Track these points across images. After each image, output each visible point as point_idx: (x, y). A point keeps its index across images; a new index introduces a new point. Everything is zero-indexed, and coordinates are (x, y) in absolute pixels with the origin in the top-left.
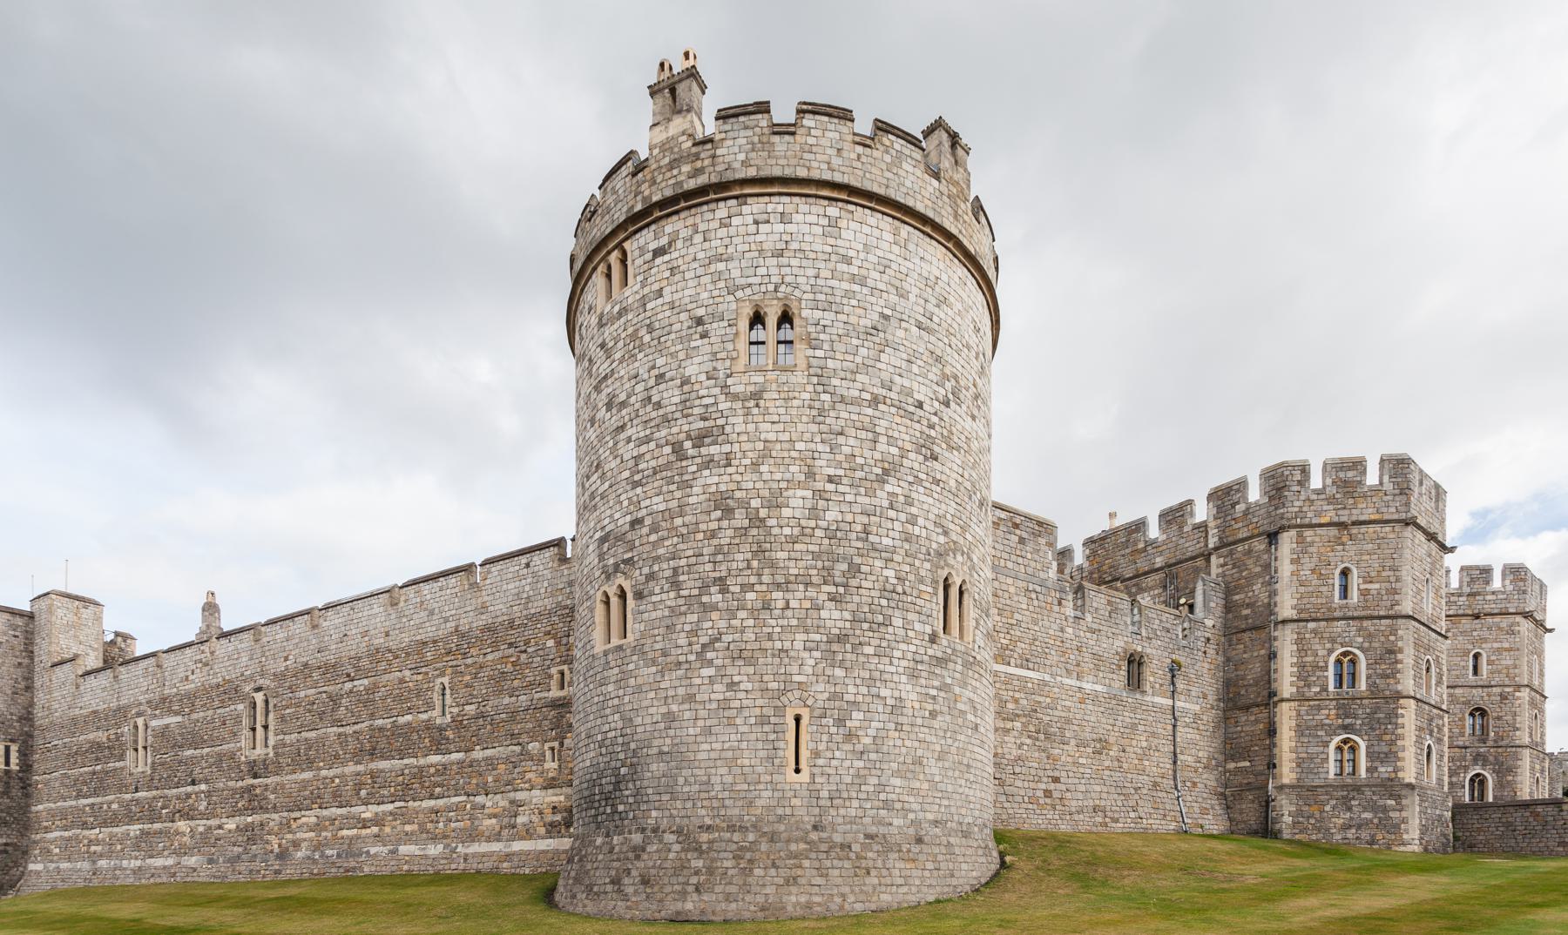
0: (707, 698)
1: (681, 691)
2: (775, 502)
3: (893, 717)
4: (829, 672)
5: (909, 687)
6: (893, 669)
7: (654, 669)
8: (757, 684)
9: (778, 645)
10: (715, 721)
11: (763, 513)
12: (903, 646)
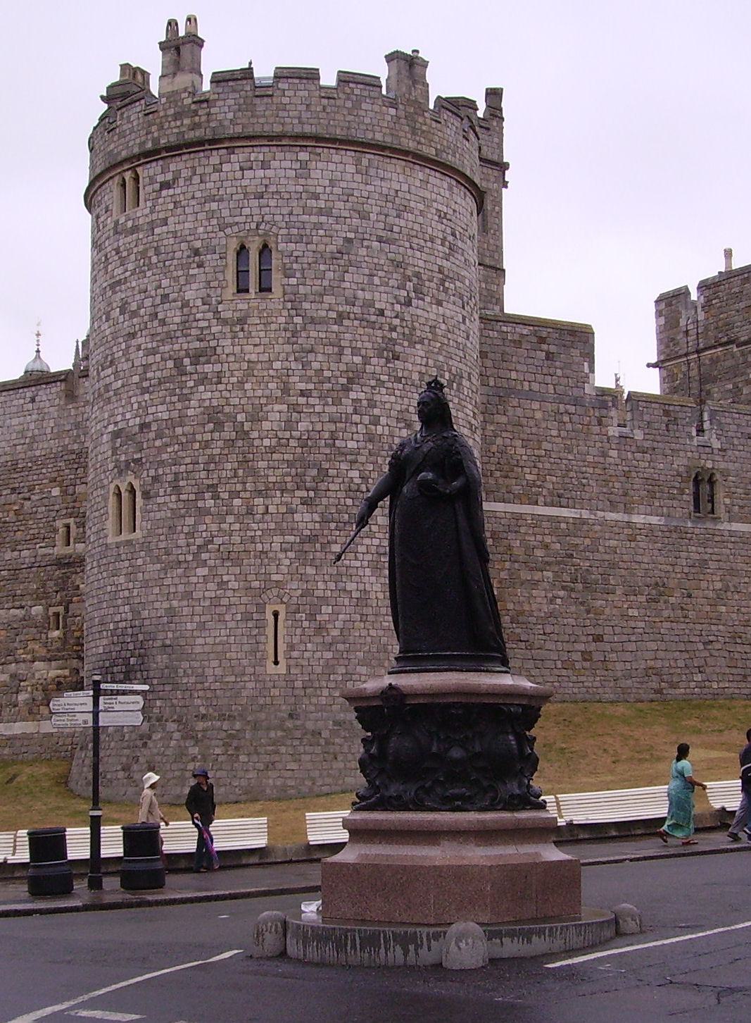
0: (201, 596)
1: (181, 588)
2: (256, 417)
5: (373, 579)
6: (358, 564)
7: (158, 566)
8: (242, 583)
10: (209, 617)
12: (367, 541)
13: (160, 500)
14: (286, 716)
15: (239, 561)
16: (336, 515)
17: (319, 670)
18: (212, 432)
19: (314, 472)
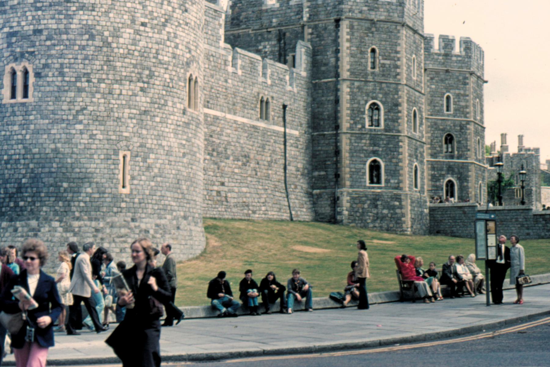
2: (116, 34)
3: (167, 157)
4: (140, 132)
5: (174, 140)
6: (167, 130)
7: (47, 121)
8: (105, 136)
9: (116, 115)
11: (110, 40)
12: (172, 117)
13: (48, 79)
14: (129, 219)
15: (104, 123)
16: (158, 100)
17: (147, 192)
18: (88, 40)
19: (147, 72)
